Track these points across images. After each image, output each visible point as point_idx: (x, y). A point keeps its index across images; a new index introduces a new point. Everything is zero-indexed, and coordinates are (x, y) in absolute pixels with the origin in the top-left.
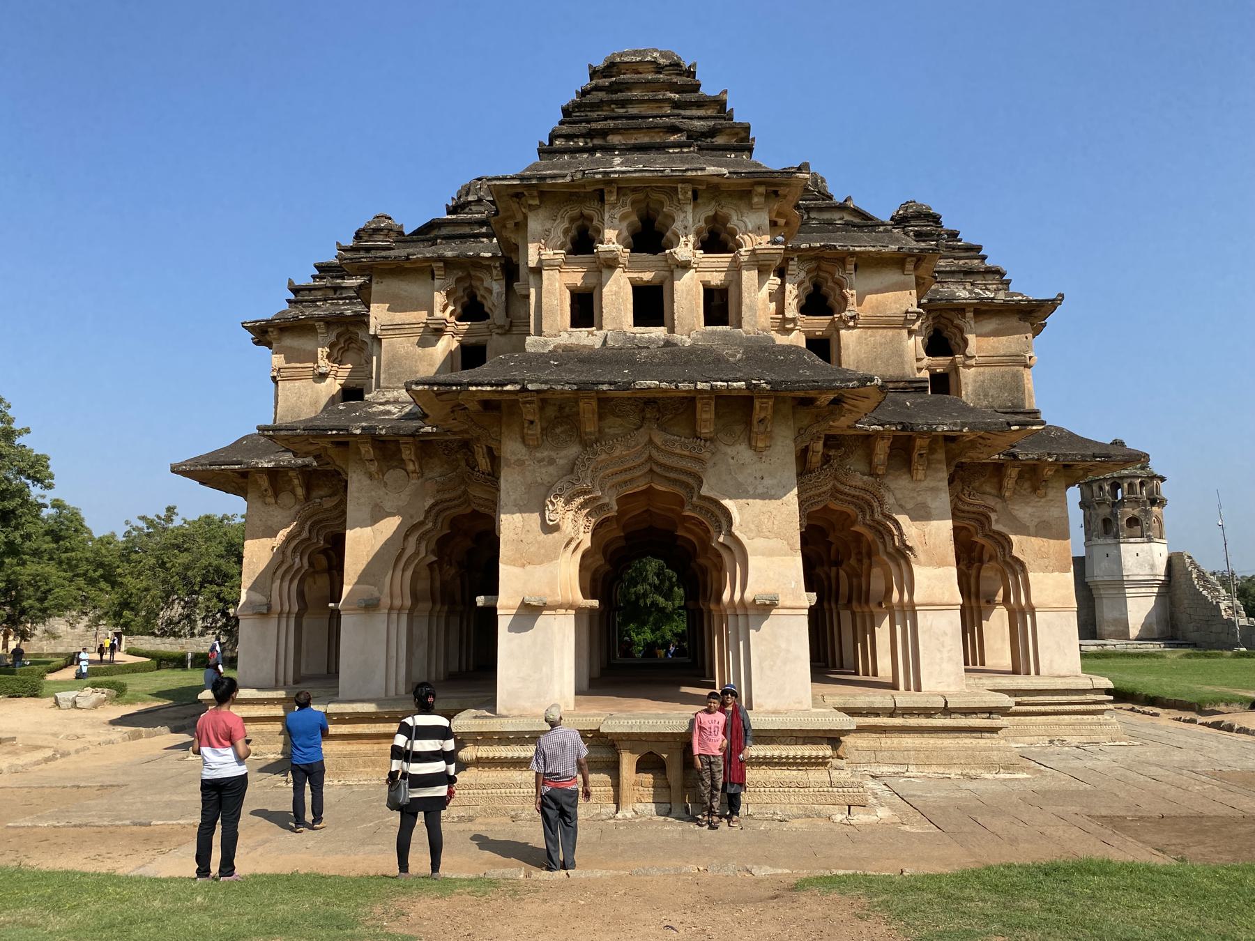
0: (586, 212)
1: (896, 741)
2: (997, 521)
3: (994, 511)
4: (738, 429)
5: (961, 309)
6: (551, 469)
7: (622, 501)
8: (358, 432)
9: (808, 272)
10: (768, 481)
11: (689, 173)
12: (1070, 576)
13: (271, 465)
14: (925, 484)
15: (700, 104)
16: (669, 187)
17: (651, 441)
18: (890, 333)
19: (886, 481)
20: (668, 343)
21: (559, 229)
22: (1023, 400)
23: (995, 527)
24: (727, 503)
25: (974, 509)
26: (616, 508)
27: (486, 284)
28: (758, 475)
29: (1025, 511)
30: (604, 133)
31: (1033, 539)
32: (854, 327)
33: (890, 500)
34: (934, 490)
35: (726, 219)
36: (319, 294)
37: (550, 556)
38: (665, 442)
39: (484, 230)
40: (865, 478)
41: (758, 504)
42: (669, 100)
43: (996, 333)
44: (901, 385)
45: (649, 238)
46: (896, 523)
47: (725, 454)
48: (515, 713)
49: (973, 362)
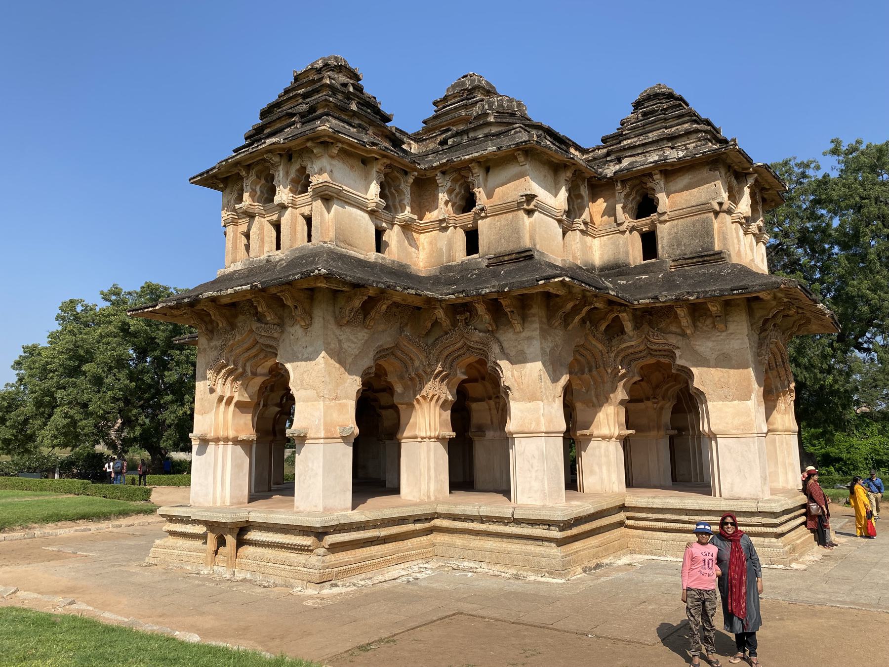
1: (482, 542)
2: (680, 357)
3: (678, 348)
5: (647, 174)
9: (454, 181)
10: (310, 349)
11: (260, 147)
14: (523, 334)
17: (251, 331)
18: (510, 216)
19: (497, 335)
22: (712, 243)
23: (679, 362)
25: (661, 347)
28: (304, 345)
29: (706, 346)
31: (713, 370)
32: (486, 217)
33: (496, 349)
34: (529, 338)
38: (258, 328)
40: (481, 334)
41: (303, 364)
42: (299, 95)
43: (688, 188)
44: (514, 256)
47: (289, 333)
48: (197, 505)
49: (665, 217)
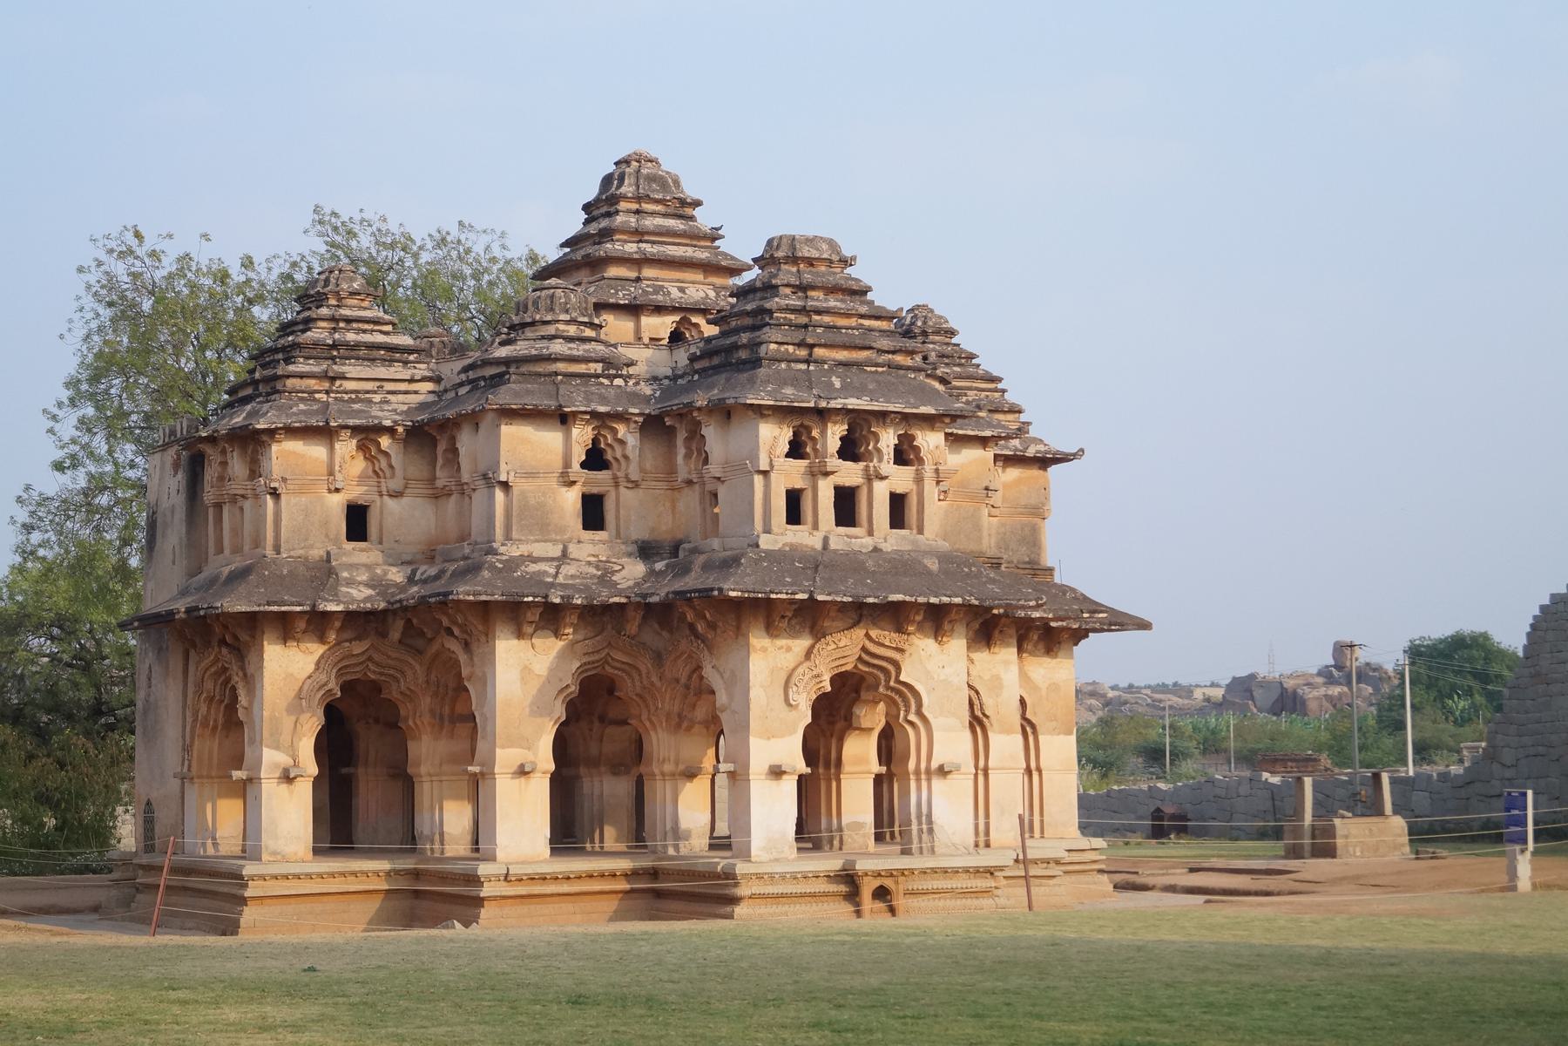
0: (807, 423)
4: (928, 625)
6: (789, 656)
7: (832, 680)
8: (557, 601)
12: (1073, 738)
13: (340, 608)
15: (877, 318)
16: (882, 416)
17: (867, 636)
20: (876, 549)
21: (786, 434)
24: (919, 687)
26: (829, 689)
27: (620, 436)
30: (812, 346)
34: (1007, 663)
35: (913, 438)
36: (312, 383)
37: (793, 732)
39: (599, 367)
45: (850, 450)
46: (977, 693)
